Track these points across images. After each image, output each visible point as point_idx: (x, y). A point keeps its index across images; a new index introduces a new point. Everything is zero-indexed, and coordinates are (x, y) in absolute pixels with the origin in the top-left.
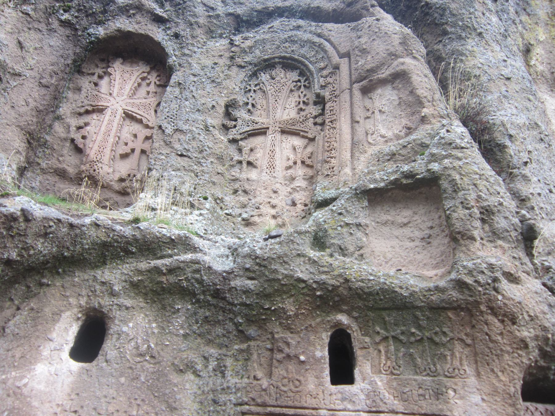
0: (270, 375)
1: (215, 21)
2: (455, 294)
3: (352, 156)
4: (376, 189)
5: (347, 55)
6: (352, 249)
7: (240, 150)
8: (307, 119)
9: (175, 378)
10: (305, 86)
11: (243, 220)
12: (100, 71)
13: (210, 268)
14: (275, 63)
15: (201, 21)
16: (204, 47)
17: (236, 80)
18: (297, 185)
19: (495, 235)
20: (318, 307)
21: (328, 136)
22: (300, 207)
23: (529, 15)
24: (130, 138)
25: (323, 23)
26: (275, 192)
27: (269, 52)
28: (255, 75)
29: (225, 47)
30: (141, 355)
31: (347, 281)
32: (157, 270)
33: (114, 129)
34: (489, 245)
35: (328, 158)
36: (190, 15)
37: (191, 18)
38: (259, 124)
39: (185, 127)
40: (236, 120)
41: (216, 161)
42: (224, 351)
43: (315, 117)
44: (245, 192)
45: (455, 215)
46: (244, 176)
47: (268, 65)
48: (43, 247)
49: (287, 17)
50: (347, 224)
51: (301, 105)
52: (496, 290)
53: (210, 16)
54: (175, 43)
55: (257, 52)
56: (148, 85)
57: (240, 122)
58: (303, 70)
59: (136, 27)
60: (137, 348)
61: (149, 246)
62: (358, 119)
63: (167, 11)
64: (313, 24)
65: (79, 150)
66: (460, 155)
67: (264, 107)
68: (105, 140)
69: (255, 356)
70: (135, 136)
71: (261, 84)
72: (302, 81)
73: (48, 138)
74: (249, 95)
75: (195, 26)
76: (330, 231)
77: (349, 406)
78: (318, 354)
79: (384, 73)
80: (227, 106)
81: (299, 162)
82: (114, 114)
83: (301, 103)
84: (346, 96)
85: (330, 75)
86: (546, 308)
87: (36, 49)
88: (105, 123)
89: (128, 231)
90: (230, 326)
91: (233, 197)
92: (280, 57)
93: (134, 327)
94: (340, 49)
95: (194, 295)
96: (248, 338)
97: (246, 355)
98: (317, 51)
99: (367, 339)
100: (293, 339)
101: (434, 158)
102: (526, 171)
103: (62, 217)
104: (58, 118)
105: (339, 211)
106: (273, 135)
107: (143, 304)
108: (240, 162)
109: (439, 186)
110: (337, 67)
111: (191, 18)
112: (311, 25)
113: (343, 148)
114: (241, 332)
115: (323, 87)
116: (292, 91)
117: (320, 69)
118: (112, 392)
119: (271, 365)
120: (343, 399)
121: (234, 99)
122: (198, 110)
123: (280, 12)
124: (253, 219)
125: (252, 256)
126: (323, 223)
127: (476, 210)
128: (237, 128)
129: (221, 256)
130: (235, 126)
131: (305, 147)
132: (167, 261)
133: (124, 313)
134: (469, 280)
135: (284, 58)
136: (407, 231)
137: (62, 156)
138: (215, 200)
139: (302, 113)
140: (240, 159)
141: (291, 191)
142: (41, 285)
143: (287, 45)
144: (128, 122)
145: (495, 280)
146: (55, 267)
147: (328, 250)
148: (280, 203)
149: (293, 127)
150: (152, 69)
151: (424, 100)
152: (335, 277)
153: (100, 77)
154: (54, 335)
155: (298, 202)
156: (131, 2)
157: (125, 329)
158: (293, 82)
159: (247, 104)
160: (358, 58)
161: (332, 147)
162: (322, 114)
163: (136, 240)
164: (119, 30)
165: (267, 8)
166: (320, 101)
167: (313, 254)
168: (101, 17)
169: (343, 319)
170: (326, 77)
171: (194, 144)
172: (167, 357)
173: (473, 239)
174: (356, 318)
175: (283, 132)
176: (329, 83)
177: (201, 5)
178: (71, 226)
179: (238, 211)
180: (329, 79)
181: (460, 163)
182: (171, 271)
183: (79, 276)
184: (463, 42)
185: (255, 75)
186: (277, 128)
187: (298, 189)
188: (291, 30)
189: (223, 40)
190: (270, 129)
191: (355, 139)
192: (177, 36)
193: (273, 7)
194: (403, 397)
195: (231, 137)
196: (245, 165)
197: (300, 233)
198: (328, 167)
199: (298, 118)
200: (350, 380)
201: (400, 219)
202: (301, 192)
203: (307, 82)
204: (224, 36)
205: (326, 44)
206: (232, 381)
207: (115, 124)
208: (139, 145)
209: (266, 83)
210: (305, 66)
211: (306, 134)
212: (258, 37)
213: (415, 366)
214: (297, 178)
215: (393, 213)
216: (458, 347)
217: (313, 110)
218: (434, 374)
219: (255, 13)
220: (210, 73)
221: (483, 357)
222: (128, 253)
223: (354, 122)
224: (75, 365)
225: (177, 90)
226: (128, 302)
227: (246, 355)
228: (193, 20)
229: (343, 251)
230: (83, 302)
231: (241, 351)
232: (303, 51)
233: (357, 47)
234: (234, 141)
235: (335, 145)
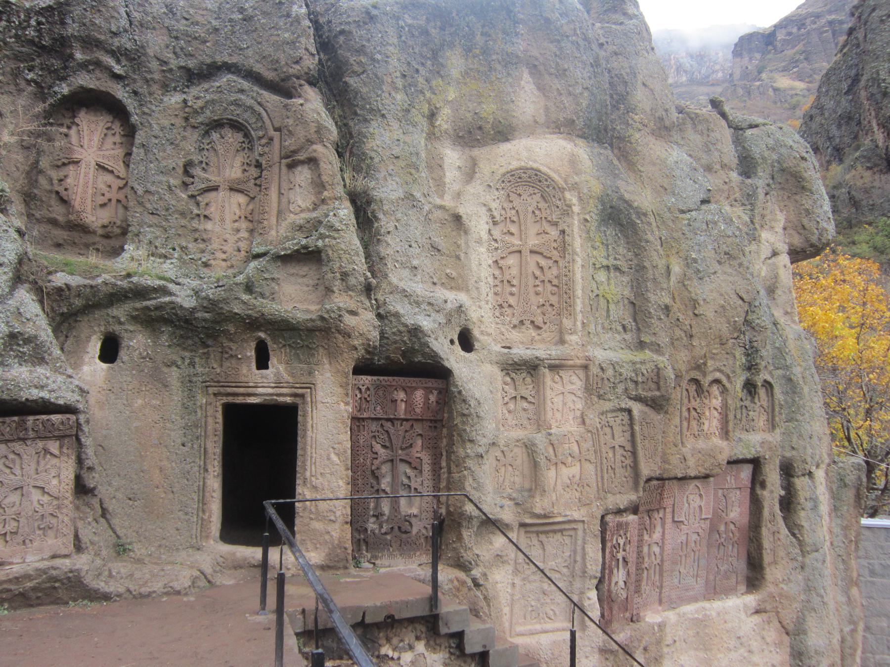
0: (221, 366)
1: (168, 75)
2: (319, 323)
3: (277, 221)
4: (285, 255)
6: (268, 294)
7: (198, 204)
9: (165, 370)
12: (67, 121)
13: (181, 306)
15: (157, 76)
17: (190, 142)
19: (349, 288)
20: (248, 329)
22: (243, 253)
23: (442, 77)
24: (105, 189)
29: (178, 106)
30: (143, 358)
31: (263, 314)
32: (147, 308)
34: (344, 294)
36: (146, 71)
37: (146, 75)
39: (153, 189)
40: (193, 177)
42: (193, 354)
43: (256, 179)
44: (203, 240)
46: (201, 227)
47: (217, 125)
48: (78, 302)
50: (266, 279)
51: (245, 167)
52: (340, 321)
53: (164, 71)
54: (135, 100)
56: (114, 135)
57: (196, 179)
59: (97, 83)
60: (141, 354)
61: (141, 293)
62: (283, 191)
63: (124, 66)
65: (64, 201)
66: (336, 235)
69: (212, 356)
70: (110, 186)
73: (36, 191)
75: (151, 83)
78: (249, 354)
79: (302, 156)
80: (185, 166)
81: (243, 217)
82: (88, 165)
84: (276, 169)
86: (372, 328)
87: (11, 112)
88: (82, 175)
89: (124, 284)
90: (196, 340)
91: (194, 244)
92: (228, 119)
93: (136, 342)
95: (173, 322)
96: (208, 346)
97: (207, 355)
99: (275, 346)
100: (234, 346)
101: (322, 237)
102: (389, 239)
103: (87, 282)
104: (41, 172)
107: (140, 329)
108: (198, 215)
109: (321, 256)
110: (271, 139)
111: (146, 75)
114: (204, 342)
115: (261, 155)
118: (129, 379)
119: (222, 361)
120: (262, 377)
122: (162, 172)
123: (228, 68)
124: (210, 262)
125: (207, 298)
127: (338, 274)
129: (188, 296)
130: (193, 183)
131: (248, 204)
132: (153, 302)
133: (130, 334)
134: (326, 316)
135: (231, 120)
136: (305, 280)
137: (51, 206)
138: (181, 248)
139: (246, 174)
140: (198, 212)
142: (76, 321)
143: (232, 107)
144: (101, 171)
145: (340, 316)
146: (84, 311)
150: (114, 117)
151: (326, 185)
152: (257, 312)
153: (69, 128)
154: (89, 350)
155: (242, 249)
156: (88, 58)
157: (131, 344)
163: (131, 289)
164: (82, 87)
165: (215, 62)
166: (258, 165)
167: (245, 297)
168: (62, 73)
169: (262, 335)
171: (161, 203)
173: (333, 292)
174: (269, 335)
175: (231, 189)
177: (155, 59)
178: (92, 287)
179: (199, 256)
180: (266, 149)
181: (334, 242)
182: (158, 308)
183: (98, 314)
184: (367, 124)
185: (207, 133)
189: (177, 93)
192: (135, 93)
194: (292, 375)
195: (190, 193)
196: (202, 218)
197: (237, 284)
200: (267, 368)
201: (302, 273)
205: (264, 114)
206: (200, 370)
207: (91, 176)
208: (114, 195)
209: (217, 142)
212: (208, 98)
213: (300, 359)
215: (297, 268)
216: (321, 350)
217: (253, 172)
218: (309, 363)
219: (205, 67)
221: (333, 355)
222: (127, 297)
223: (280, 194)
224: (105, 366)
225: (142, 150)
226: (131, 328)
227: (207, 355)
228: (149, 77)
229: (262, 295)
230: (103, 329)
231: (204, 353)
234: (192, 197)
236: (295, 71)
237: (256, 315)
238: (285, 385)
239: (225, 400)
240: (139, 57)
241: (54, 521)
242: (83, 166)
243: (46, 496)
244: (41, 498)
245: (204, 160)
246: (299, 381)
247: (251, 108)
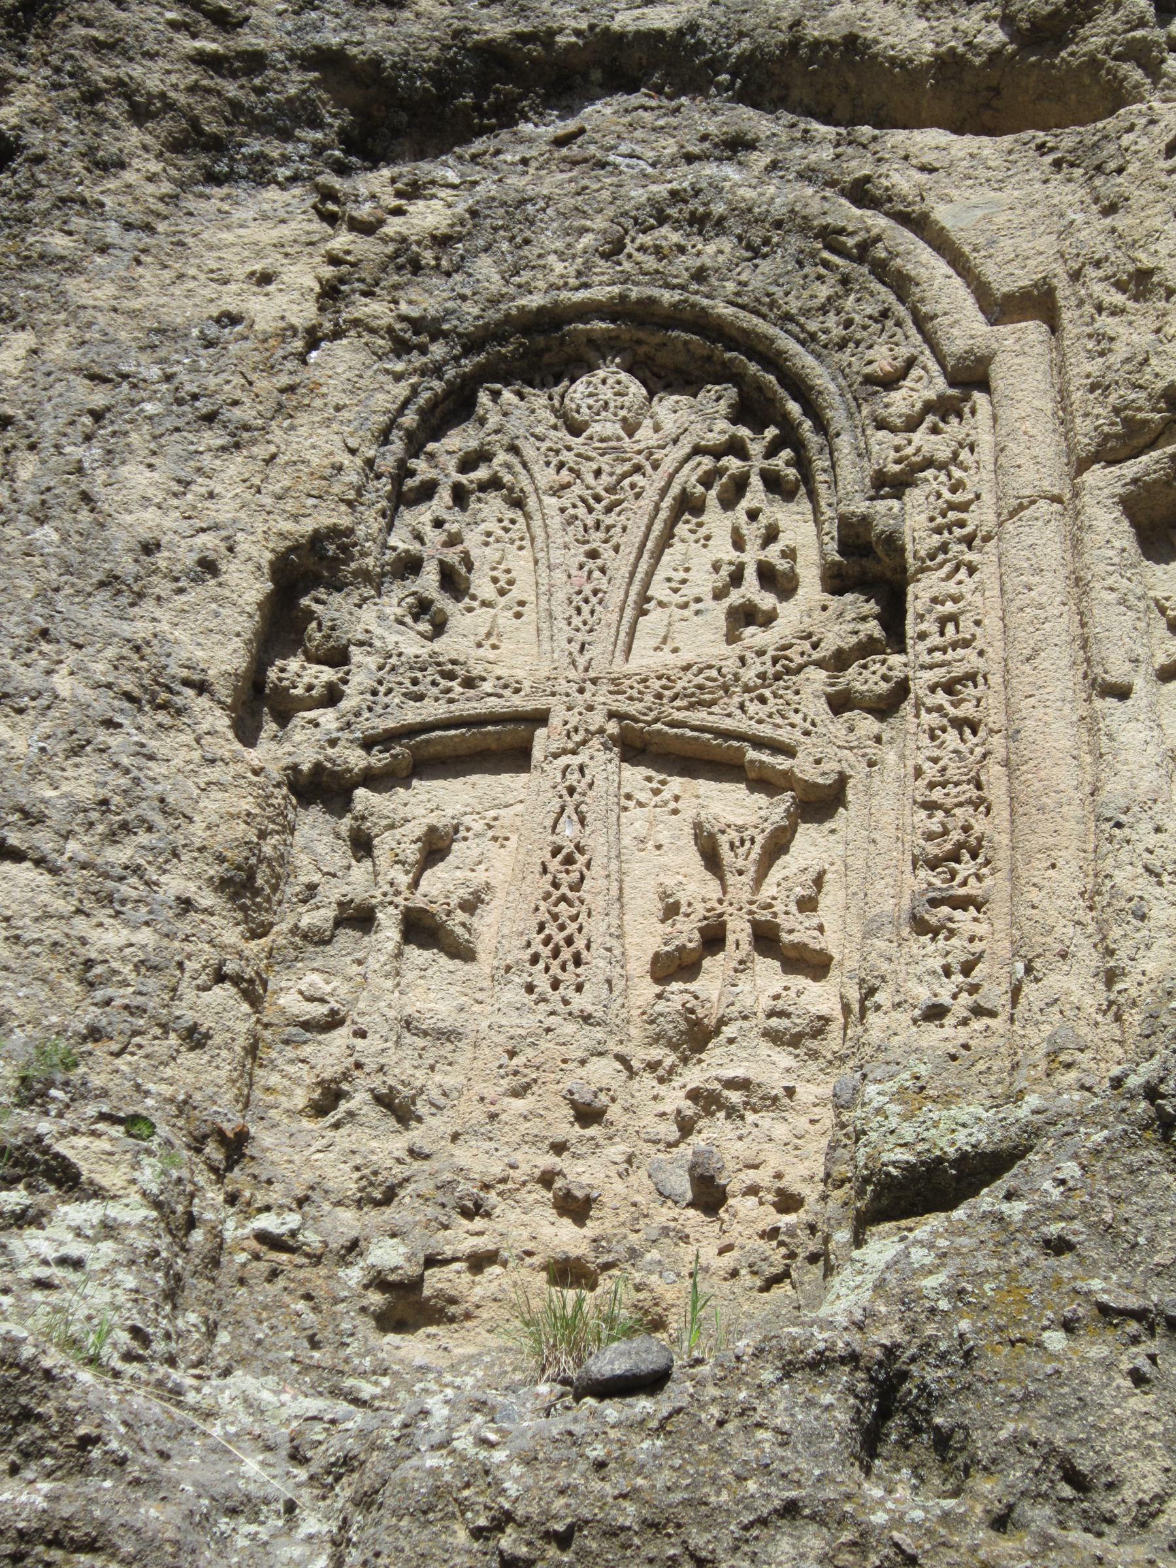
5: (1038, 304)
8: (784, 669)
10: (773, 483)
11: (379, 1281)
14: (591, 341)
16: (161, 227)
18: (729, 1073)
21: (930, 771)
25: (879, 124)
27: (559, 272)
35: (934, 903)
38: (487, 687)
40: (338, 657)
41: (207, 899)
43: (839, 661)
47: (541, 350)
49: (659, 90)
51: (751, 590)
58: (760, 388)
64: (820, 129)
67: (515, 593)
71: (502, 457)
72: (756, 449)
81: (739, 930)
83: (750, 574)
85: (930, 419)
92: (617, 310)
94: (990, 271)
98: (845, 281)
105: (1054, 1229)
106: (575, 761)
108: (359, 918)
112: (806, 137)
113: (1036, 842)
115: (891, 485)
116: (689, 505)
117: (869, 380)
121: (335, 532)
124: (436, 1281)
126: (944, 1305)
128: (344, 705)
131: (778, 845)
141: (689, 1108)
143: (669, 236)
147: (985, 1485)
148: (619, 1186)
149: (699, 716)
158: (697, 450)
160: (1106, 323)
161: (956, 836)
162: (896, 639)
170: (912, 425)
175: (635, 747)
176: (929, 463)
186: (597, 719)
187: (735, 1097)
188: (690, 158)
189: (272, 193)
190: (555, 721)
191: (1114, 790)
193: (578, 33)
198: (937, 963)
199: (730, 666)
202: (750, 1117)
203: (786, 454)
204: (282, 173)
205: (905, 238)
210: (773, 361)
211: (782, 763)
212: (487, 188)
214: (729, 1031)
220: (194, 369)
232: (759, 277)
233: (1098, 264)
234: (321, 788)
235: (978, 829)
247: (794, 222)
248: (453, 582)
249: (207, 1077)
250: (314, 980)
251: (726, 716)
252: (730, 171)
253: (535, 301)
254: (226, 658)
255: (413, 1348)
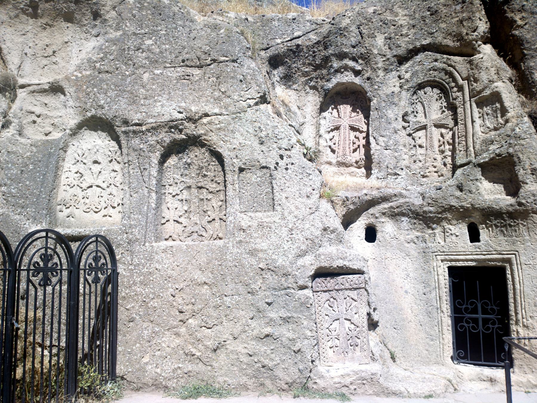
6: (474, 191)
7: (413, 139)
15: (380, 65)
26: (435, 159)
28: (415, 93)
32: (391, 207)
33: (347, 136)
40: (409, 123)
45: (519, 173)
47: (421, 86)
53: (384, 61)
55: (415, 79)
68: (345, 144)
74: (413, 106)
75: (377, 70)
76: (464, 184)
77: (478, 250)
80: (403, 117)
94: (462, 75)
134: (524, 201)
143: (432, 72)
159: (413, 112)
163: (381, 197)
172: (402, 238)
182: (397, 207)
189: (393, 72)
196: (418, 147)
200: (479, 241)
207: (347, 134)
213: (504, 234)
236: (474, 37)
237: (468, 206)
238: (494, 252)
239: (450, 264)
240: (369, 56)
241: (358, 341)
242: (343, 129)
243: (353, 325)
244: (350, 326)
245: (415, 110)
246: (505, 249)
247: (443, 69)
248: (417, 113)
249: (406, 163)
250: (412, 152)
251: (443, 122)
252: (437, 63)
253: (420, 82)
254: (400, 127)
255: (424, 179)
